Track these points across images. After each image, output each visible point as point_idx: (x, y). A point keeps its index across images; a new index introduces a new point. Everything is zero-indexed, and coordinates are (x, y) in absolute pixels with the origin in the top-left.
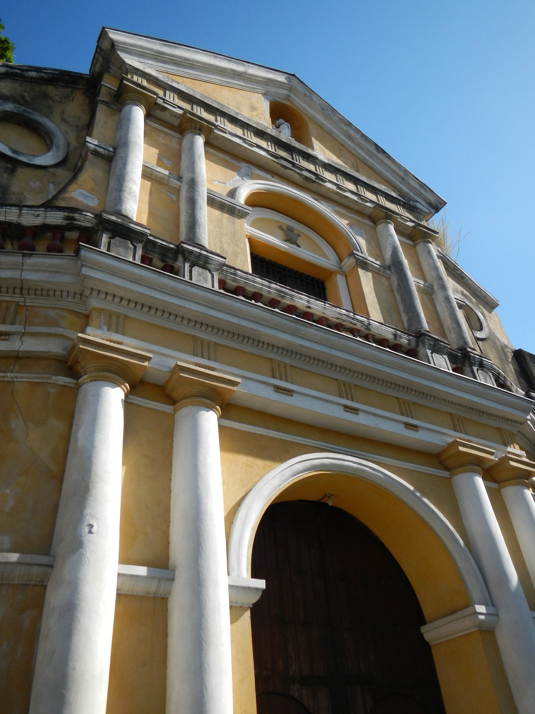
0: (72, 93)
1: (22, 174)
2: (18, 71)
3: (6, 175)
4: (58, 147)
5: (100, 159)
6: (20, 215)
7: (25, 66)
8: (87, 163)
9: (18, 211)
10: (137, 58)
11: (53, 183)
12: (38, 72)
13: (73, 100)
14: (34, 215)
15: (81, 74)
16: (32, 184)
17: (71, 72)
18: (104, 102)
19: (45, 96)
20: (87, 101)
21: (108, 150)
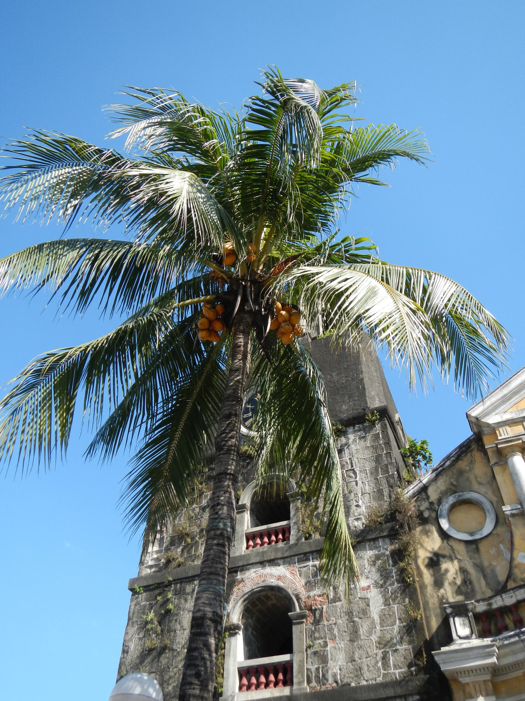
0: (472, 456)
1: (482, 547)
2: (441, 468)
3: (476, 556)
4: (489, 512)
5: (517, 517)
6: (503, 600)
7: (441, 462)
8: (513, 527)
9: (500, 598)
10: (494, 413)
11: (501, 542)
12: (449, 459)
13: (475, 461)
14: (509, 597)
15: (469, 438)
16: (491, 552)
17: (464, 442)
18: (495, 463)
19: (461, 473)
20: (483, 455)
21: (519, 509)
